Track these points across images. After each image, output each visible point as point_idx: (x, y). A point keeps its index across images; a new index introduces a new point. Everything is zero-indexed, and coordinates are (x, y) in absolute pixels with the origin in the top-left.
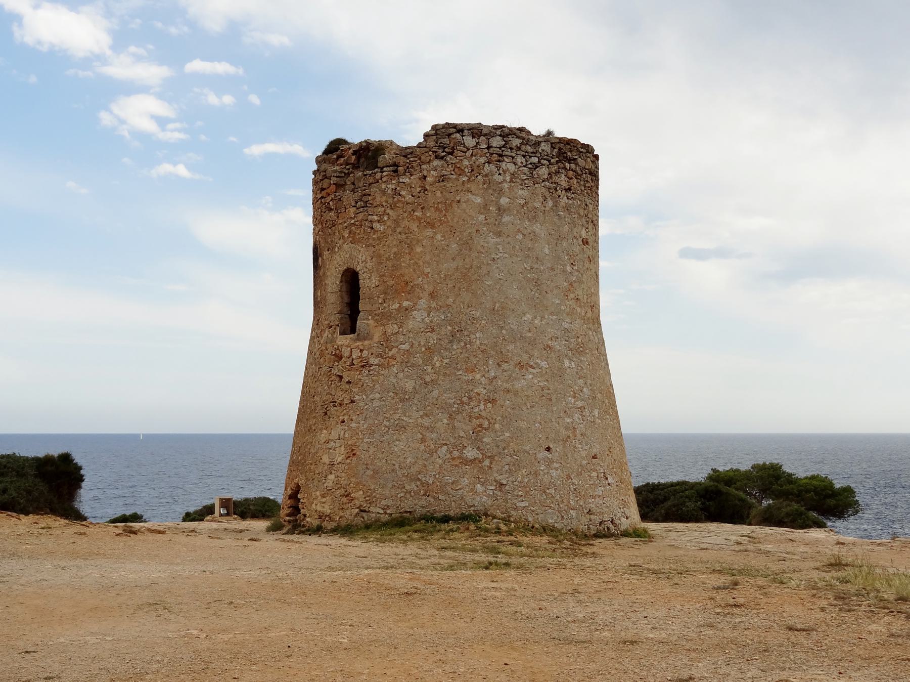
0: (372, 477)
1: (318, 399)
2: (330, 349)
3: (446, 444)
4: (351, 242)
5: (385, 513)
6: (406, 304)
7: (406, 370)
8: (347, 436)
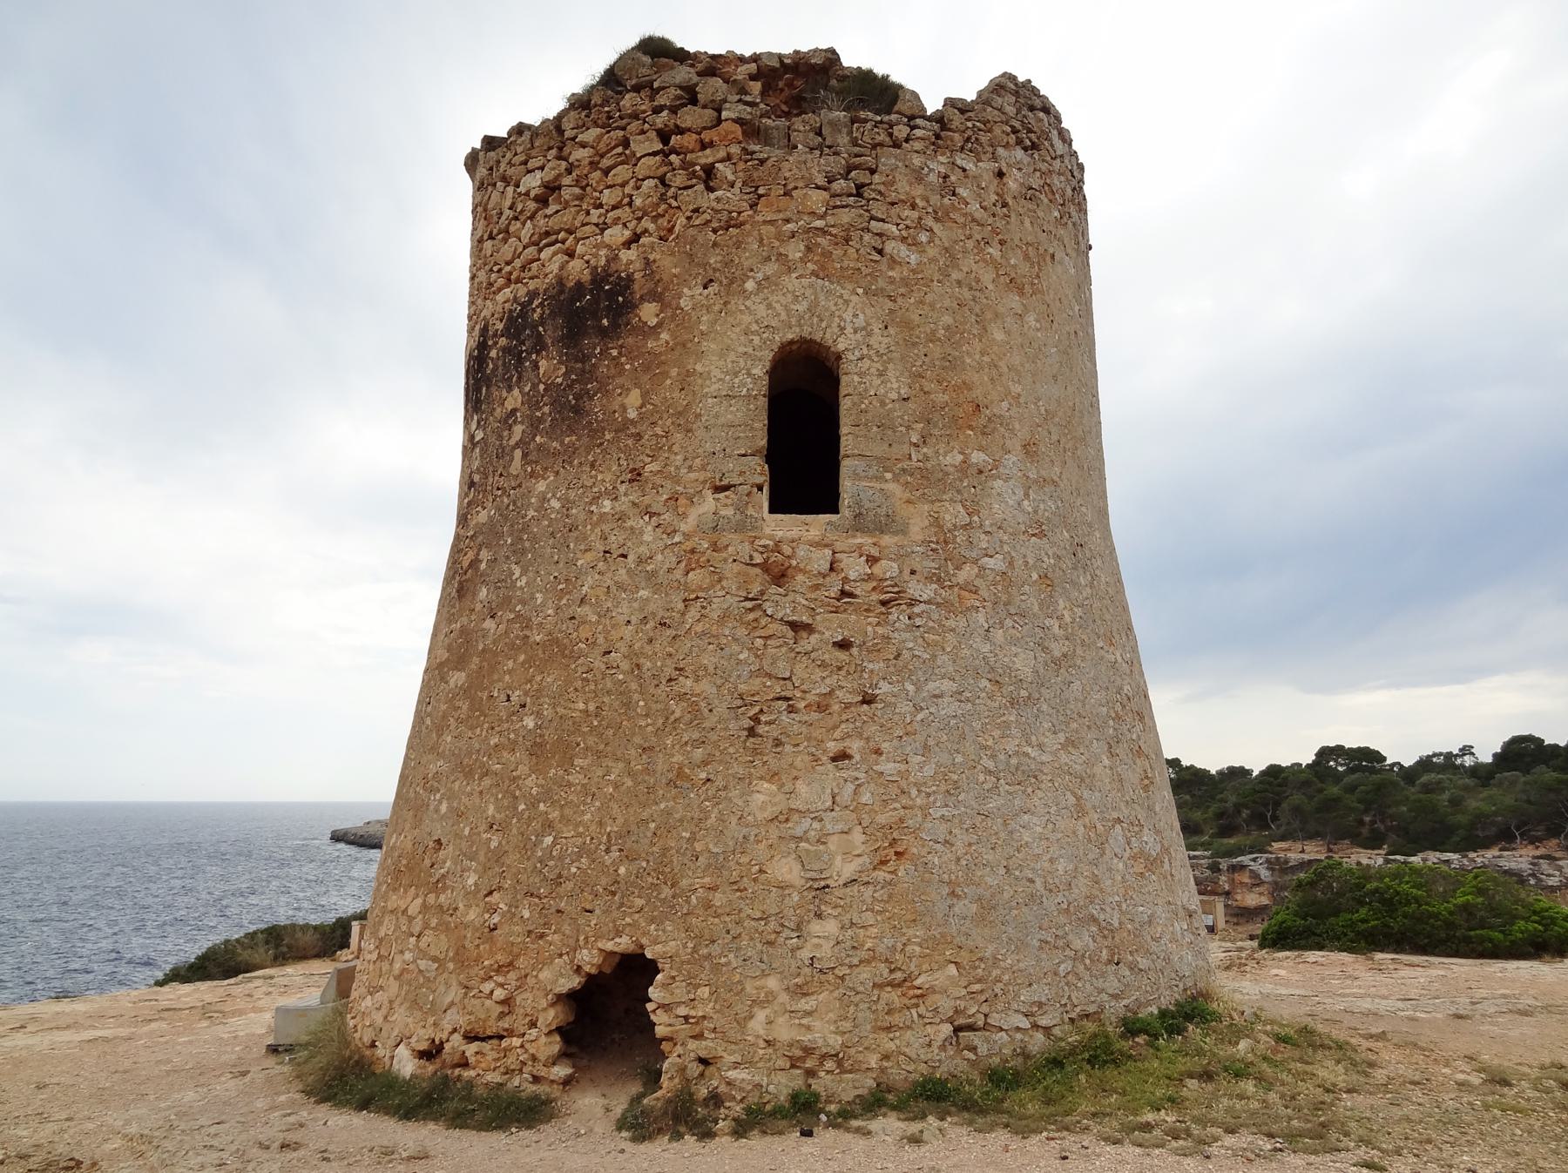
0: (980, 919)
1: (706, 686)
2: (739, 547)
3: (1119, 821)
4: (813, 273)
5: (1035, 1026)
6: (977, 457)
7: (1009, 623)
8: (866, 798)
